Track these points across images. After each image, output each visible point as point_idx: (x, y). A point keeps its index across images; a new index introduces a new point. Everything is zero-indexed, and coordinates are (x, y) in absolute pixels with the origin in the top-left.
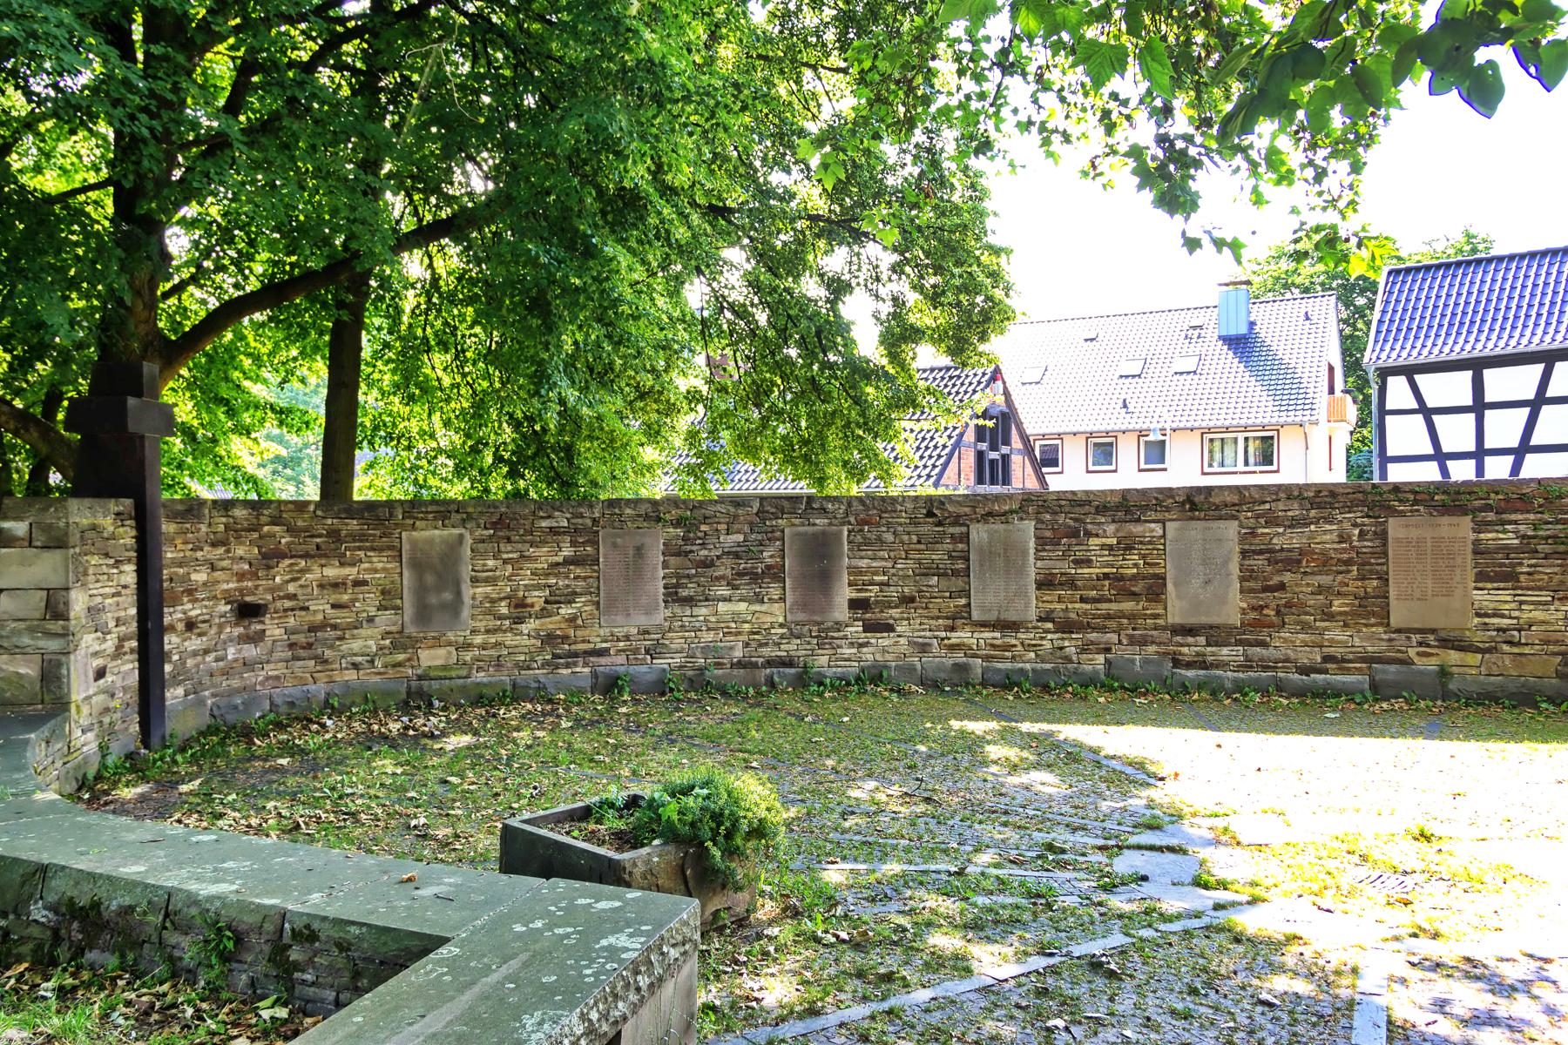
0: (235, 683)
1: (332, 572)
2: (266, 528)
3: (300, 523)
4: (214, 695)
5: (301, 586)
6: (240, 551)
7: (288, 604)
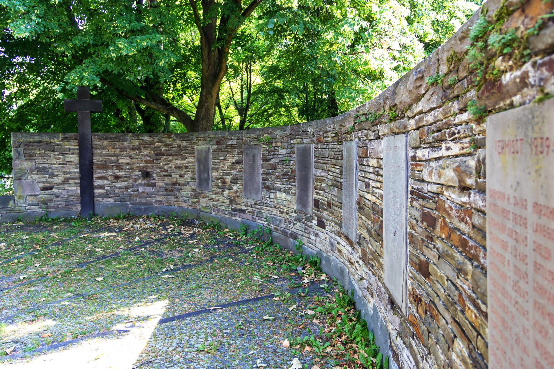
0: (143, 201)
1: (178, 162)
2: (156, 144)
3: (168, 142)
4: (131, 204)
5: (170, 167)
6: (146, 152)
7: (165, 174)
